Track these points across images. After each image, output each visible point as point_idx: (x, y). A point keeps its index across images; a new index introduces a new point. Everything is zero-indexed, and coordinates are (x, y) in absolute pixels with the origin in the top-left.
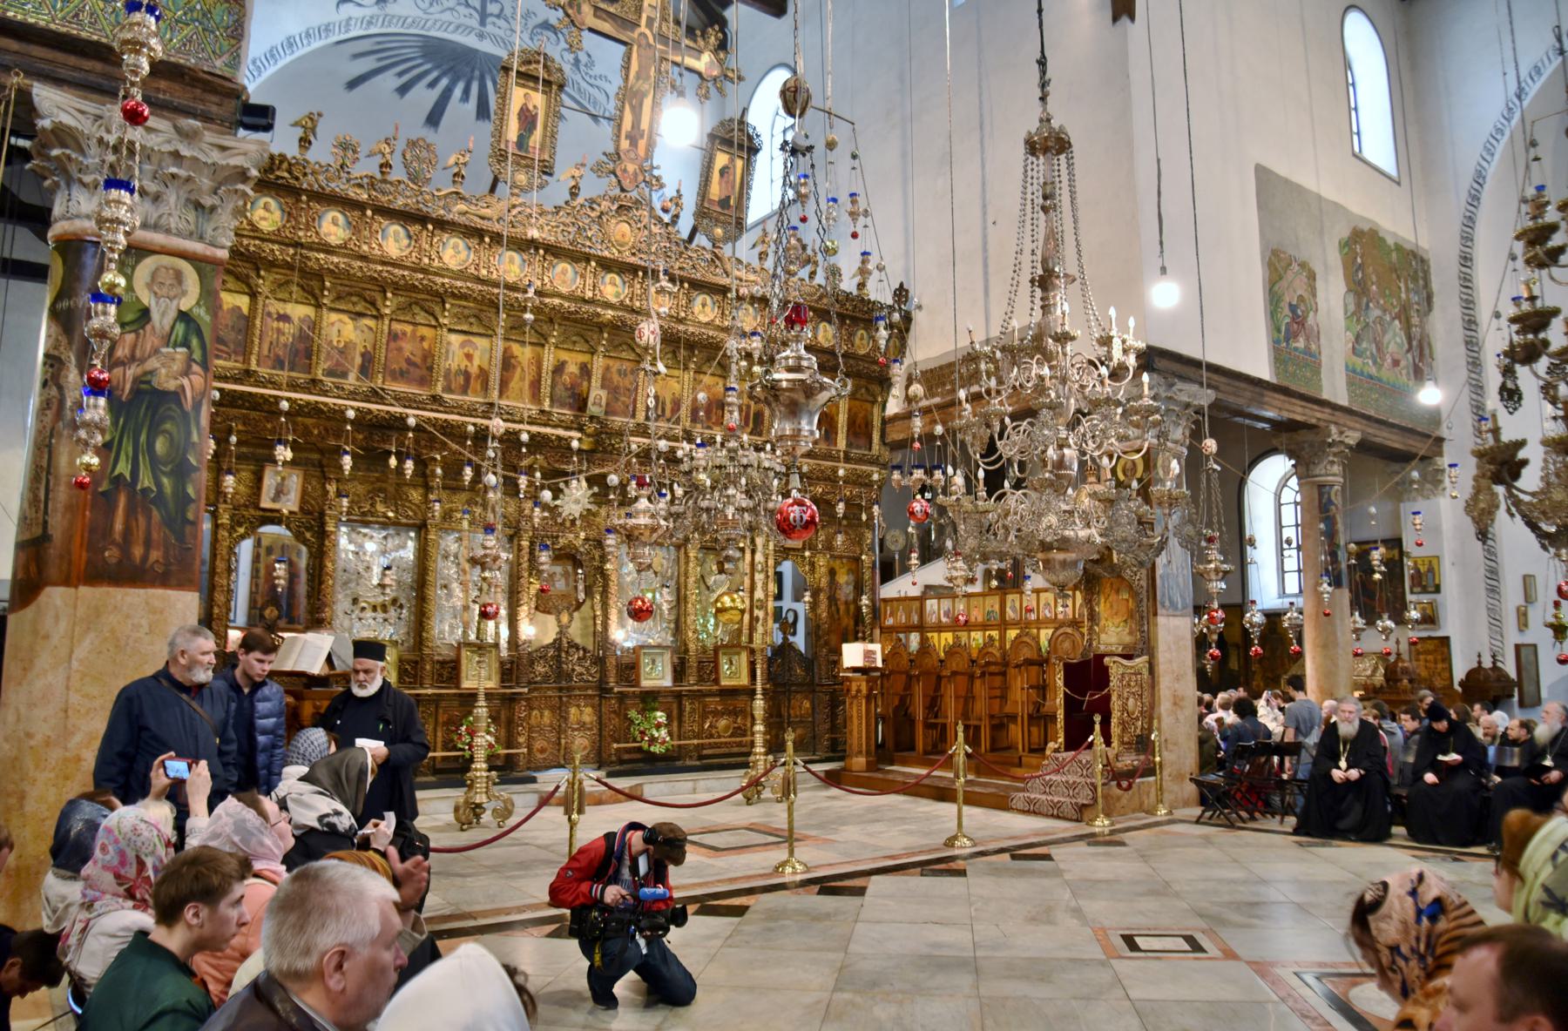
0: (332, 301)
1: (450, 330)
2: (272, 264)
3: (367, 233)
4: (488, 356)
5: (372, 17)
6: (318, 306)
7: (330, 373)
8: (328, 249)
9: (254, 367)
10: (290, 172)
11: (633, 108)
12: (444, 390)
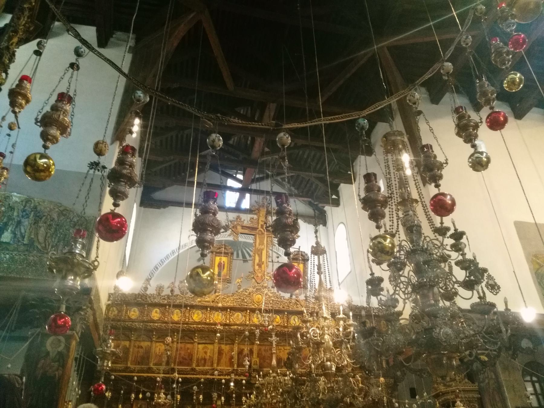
0: (156, 339)
1: (199, 344)
2: (136, 330)
3: (167, 314)
4: (212, 351)
6: (151, 341)
7: (155, 364)
8: (153, 321)
9: (129, 365)
10: (141, 298)
11: (258, 255)
12: (196, 366)
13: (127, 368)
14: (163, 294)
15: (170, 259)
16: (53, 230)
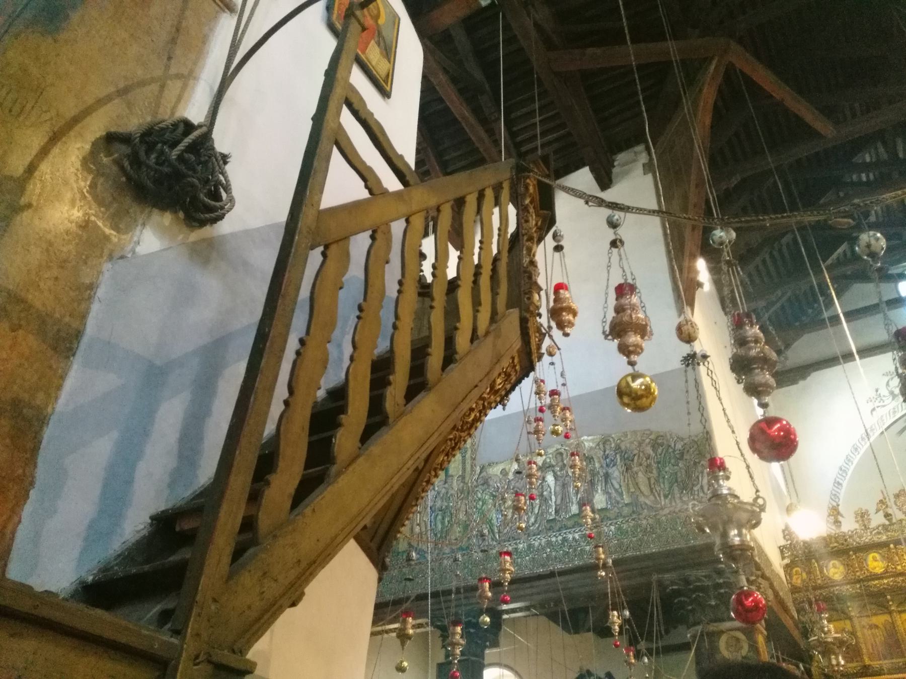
0: (898, 607)
5: (894, 409)
6: (890, 613)
9: (867, 662)
10: (837, 542)
13: (866, 667)
14: (873, 524)
15: (855, 462)
16: (655, 471)
